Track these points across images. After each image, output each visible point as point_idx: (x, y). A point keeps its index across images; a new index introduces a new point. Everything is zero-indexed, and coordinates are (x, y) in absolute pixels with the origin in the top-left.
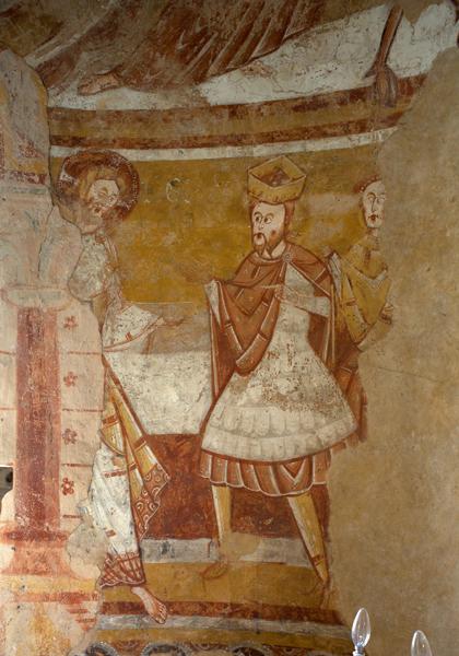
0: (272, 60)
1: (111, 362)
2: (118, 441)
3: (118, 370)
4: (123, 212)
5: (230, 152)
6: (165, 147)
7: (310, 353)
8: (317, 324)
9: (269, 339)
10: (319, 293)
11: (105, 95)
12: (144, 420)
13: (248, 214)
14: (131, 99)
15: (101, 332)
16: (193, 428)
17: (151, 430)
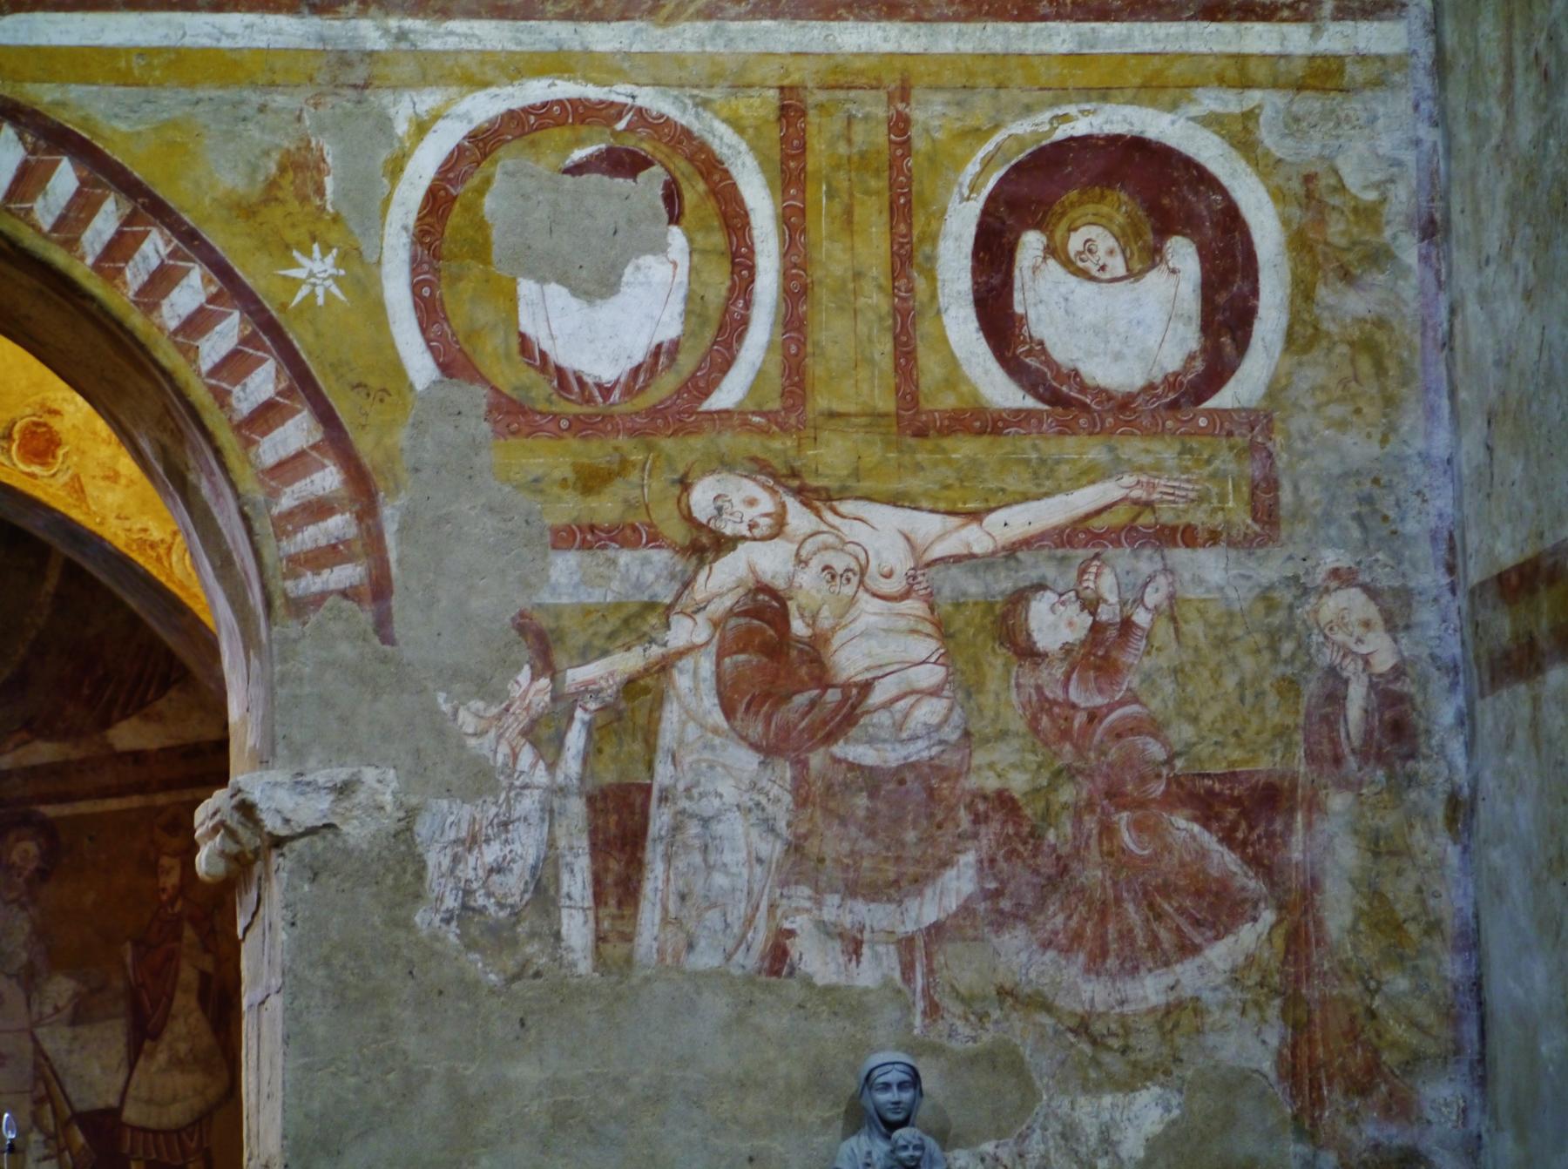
0: (161, 705)
1: (40, 1037)
2: (49, 1121)
3: (48, 1046)
4: (43, 875)
5: (136, 801)
6: (81, 799)
7: (198, 1014)
8: (204, 977)
9: (171, 1000)
10: (206, 950)
11: (20, 752)
12: (73, 1098)
13: (153, 869)
14: (45, 752)
15: (29, 1005)
16: (113, 1101)
17: (81, 1107)
